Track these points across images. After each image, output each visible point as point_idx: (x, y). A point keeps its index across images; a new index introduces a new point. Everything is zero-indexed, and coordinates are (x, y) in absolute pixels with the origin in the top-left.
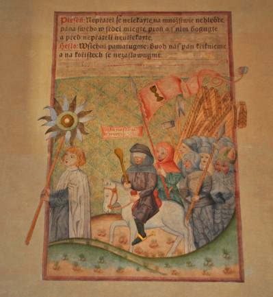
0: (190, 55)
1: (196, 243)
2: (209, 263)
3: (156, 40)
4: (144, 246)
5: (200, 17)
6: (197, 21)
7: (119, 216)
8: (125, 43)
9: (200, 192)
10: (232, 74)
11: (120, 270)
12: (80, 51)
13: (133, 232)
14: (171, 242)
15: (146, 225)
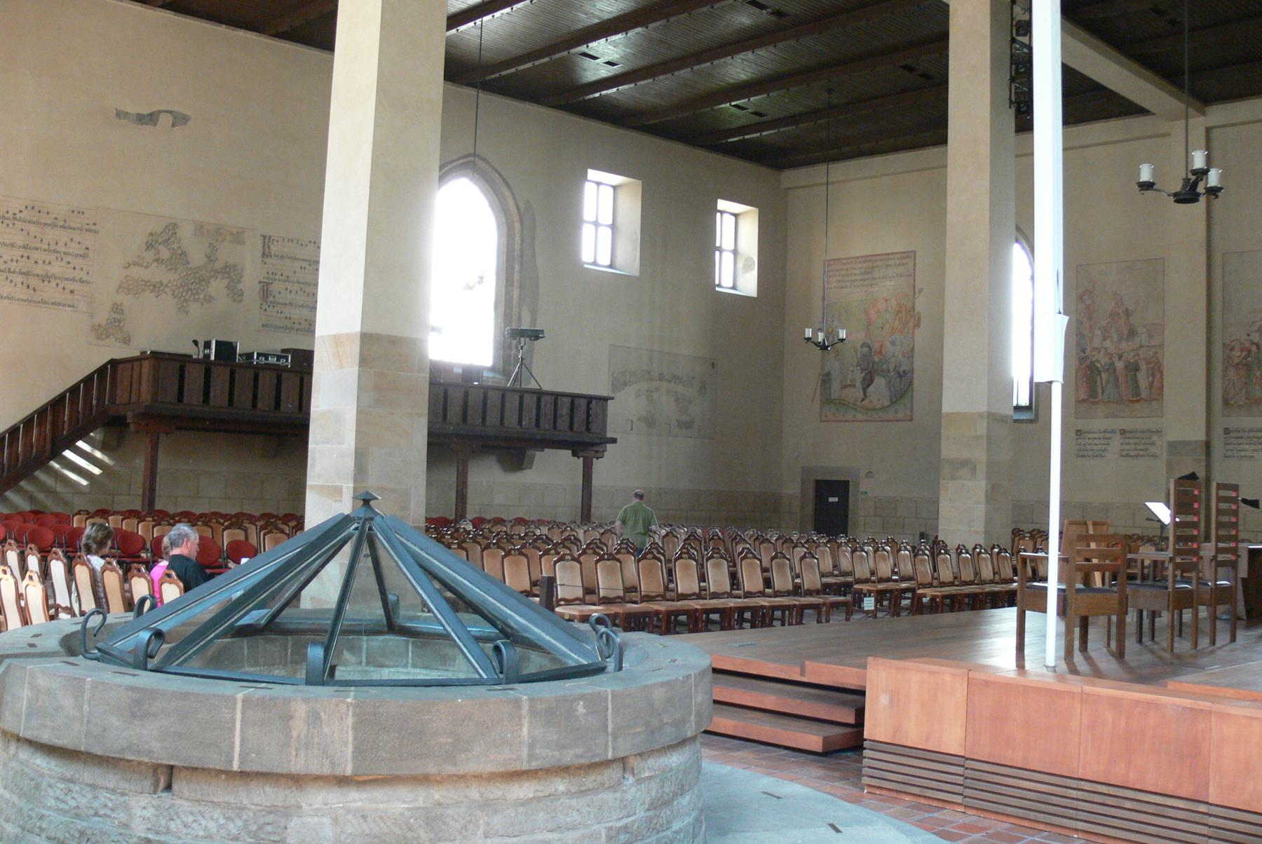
0: (893, 283)
1: (891, 400)
2: (896, 411)
3: (876, 274)
4: (866, 402)
5: (899, 256)
6: (898, 259)
7: (854, 386)
8: (859, 277)
9: (895, 370)
10: (914, 294)
11: (854, 416)
12: (836, 284)
13: (861, 395)
14: (879, 400)
15: (868, 391)
